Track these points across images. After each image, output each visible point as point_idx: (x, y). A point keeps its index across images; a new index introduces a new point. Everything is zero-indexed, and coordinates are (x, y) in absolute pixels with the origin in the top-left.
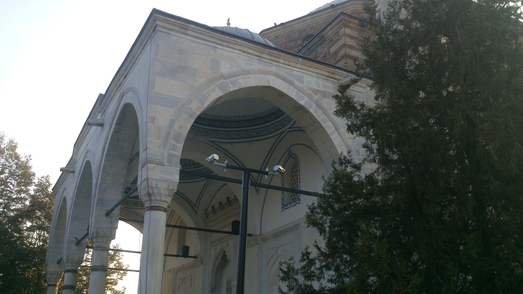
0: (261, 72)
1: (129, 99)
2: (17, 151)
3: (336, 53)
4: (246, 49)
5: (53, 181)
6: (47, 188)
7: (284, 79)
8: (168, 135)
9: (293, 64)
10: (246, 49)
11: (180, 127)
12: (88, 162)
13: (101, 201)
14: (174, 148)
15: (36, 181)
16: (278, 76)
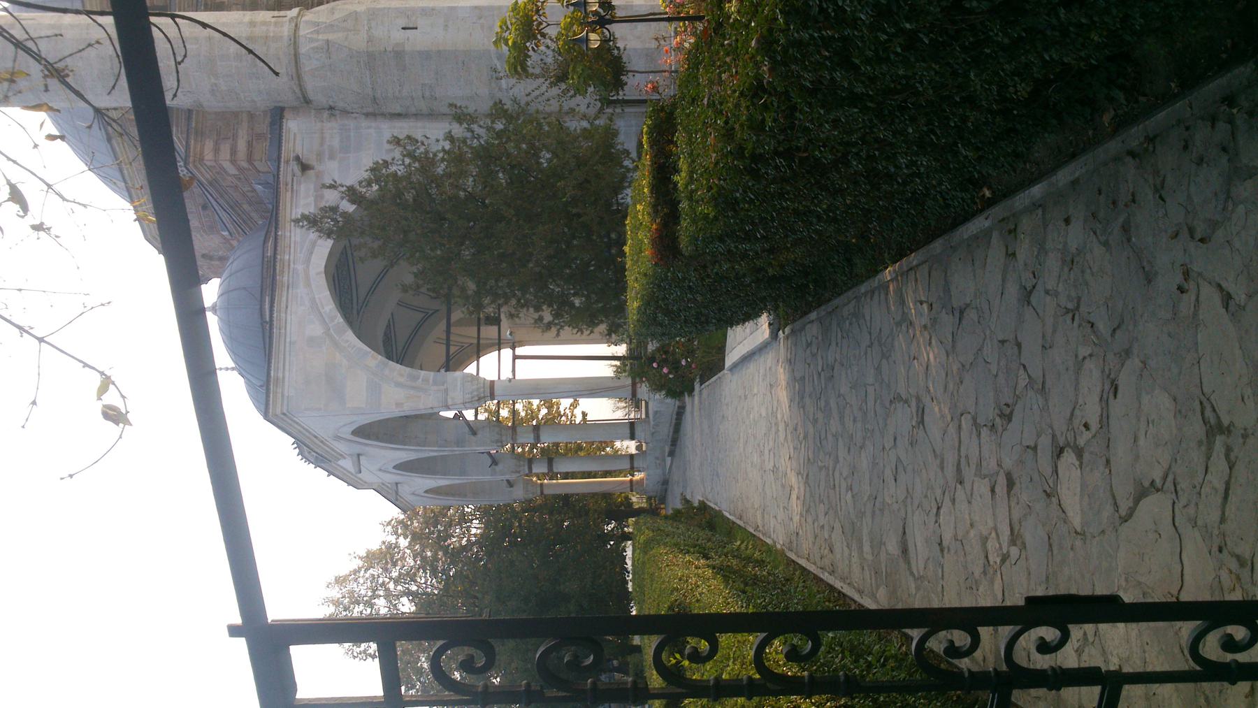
0: (308, 284)
2: (344, 572)
3: (239, 169)
4: (283, 305)
5: (395, 512)
6: (401, 522)
8: (413, 388)
9: (287, 241)
10: (283, 305)
11: (402, 375)
12: (395, 467)
13: (459, 443)
14: (426, 380)
15: (392, 539)
16: (308, 261)
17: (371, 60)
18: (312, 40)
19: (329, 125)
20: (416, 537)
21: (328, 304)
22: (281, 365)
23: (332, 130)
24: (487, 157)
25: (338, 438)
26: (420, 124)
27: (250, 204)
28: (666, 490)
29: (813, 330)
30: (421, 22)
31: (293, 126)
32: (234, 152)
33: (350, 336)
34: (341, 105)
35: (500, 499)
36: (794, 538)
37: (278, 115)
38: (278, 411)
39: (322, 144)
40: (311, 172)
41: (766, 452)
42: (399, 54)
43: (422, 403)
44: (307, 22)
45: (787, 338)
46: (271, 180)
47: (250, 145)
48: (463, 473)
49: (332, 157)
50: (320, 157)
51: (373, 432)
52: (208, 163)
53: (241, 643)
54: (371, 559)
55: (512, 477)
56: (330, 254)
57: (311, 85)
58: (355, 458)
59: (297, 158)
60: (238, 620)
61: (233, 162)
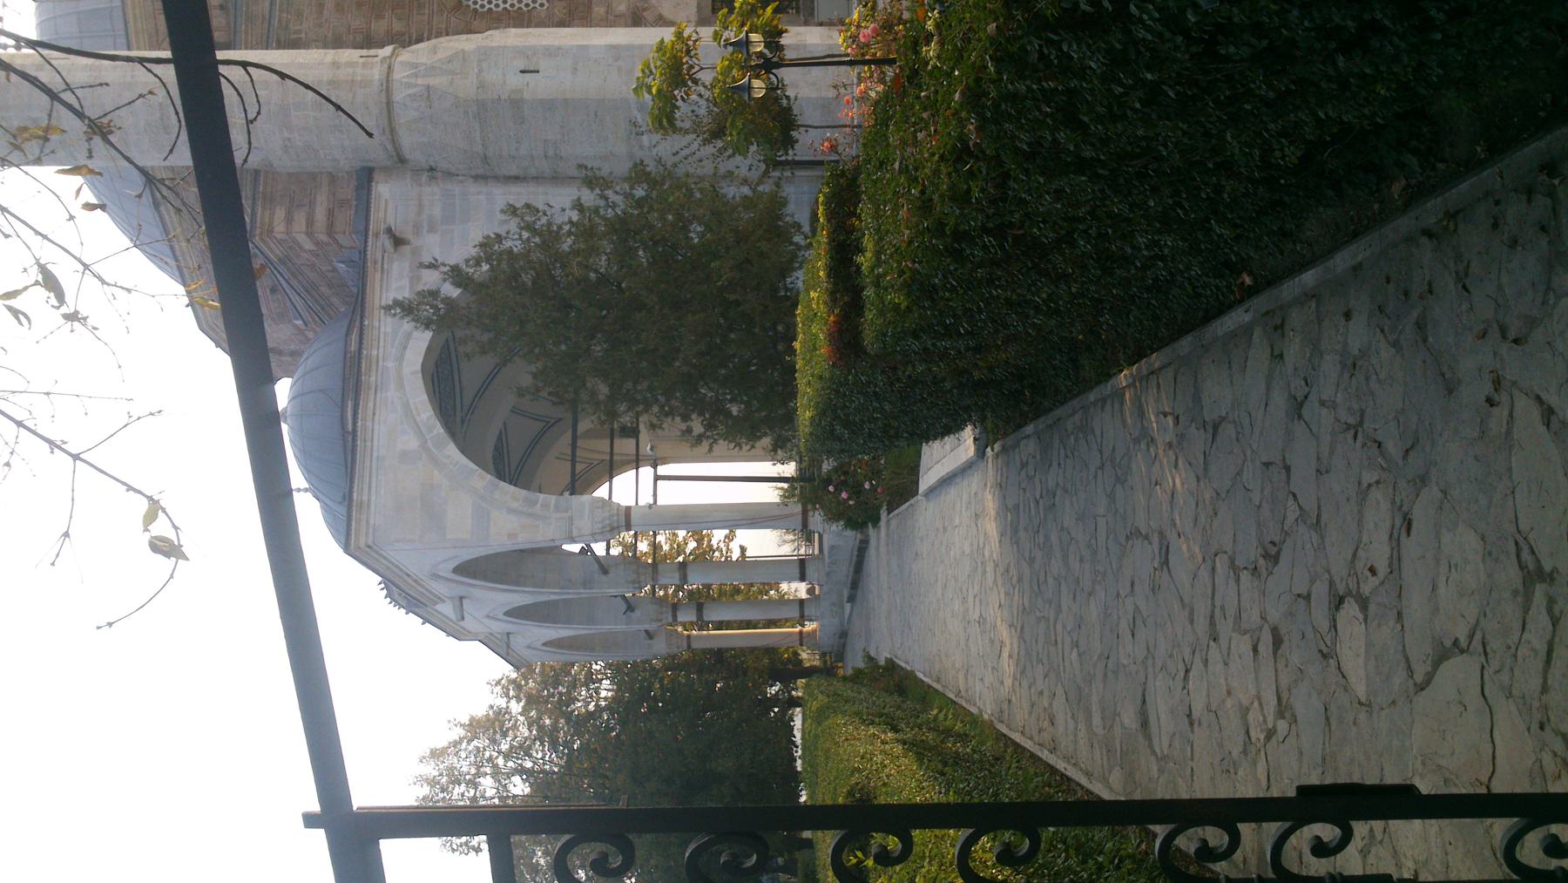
1: (446, 569)
2: (441, 743)
3: (317, 244)
5: (505, 669)
6: (514, 681)
7: (405, 348)
8: (531, 515)
9: (375, 332)
13: (586, 584)
15: (502, 702)
17: (483, 109)
18: (409, 85)
19: (427, 190)
20: (532, 701)
21: (425, 411)
22: (366, 487)
23: (433, 194)
24: (624, 230)
25: (435, 577)
26: (541, 189)
27: (330, 286)
28: (844, 646)
29: (1030, 447)
30: (543, 65)
31: (384, 190)
32: (310, 222)
33: (452, 450)
34: (443, 165)
35: (636, 655)
36: (1005, 706)
37: (366, 176)
38: (362, 544)
39: (419, 213)
40: (406, 249)
41: (971, 599)
42: (516, 103)
43: (540, 534)
44: (402, 63)
45: (997, 456)
46: (356, 257)
47: (330, 213)
48: (590, 620)
49: (432, 230)
50: (417, 228)
51: (479, 569)
52: (279, 236)
53: (320, 835)
54: (475, 727)
55: (651, 627)
56: (429, 349)
57: (407, 141)
58: (457, 602)
59: (389, 231)
60: (315, 807)
61: (310, 234)
